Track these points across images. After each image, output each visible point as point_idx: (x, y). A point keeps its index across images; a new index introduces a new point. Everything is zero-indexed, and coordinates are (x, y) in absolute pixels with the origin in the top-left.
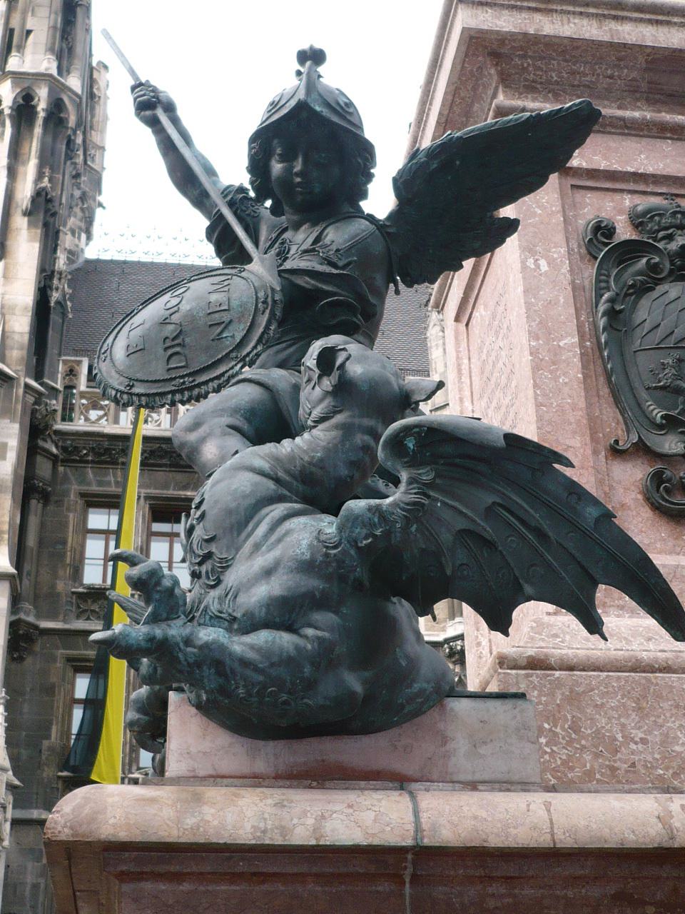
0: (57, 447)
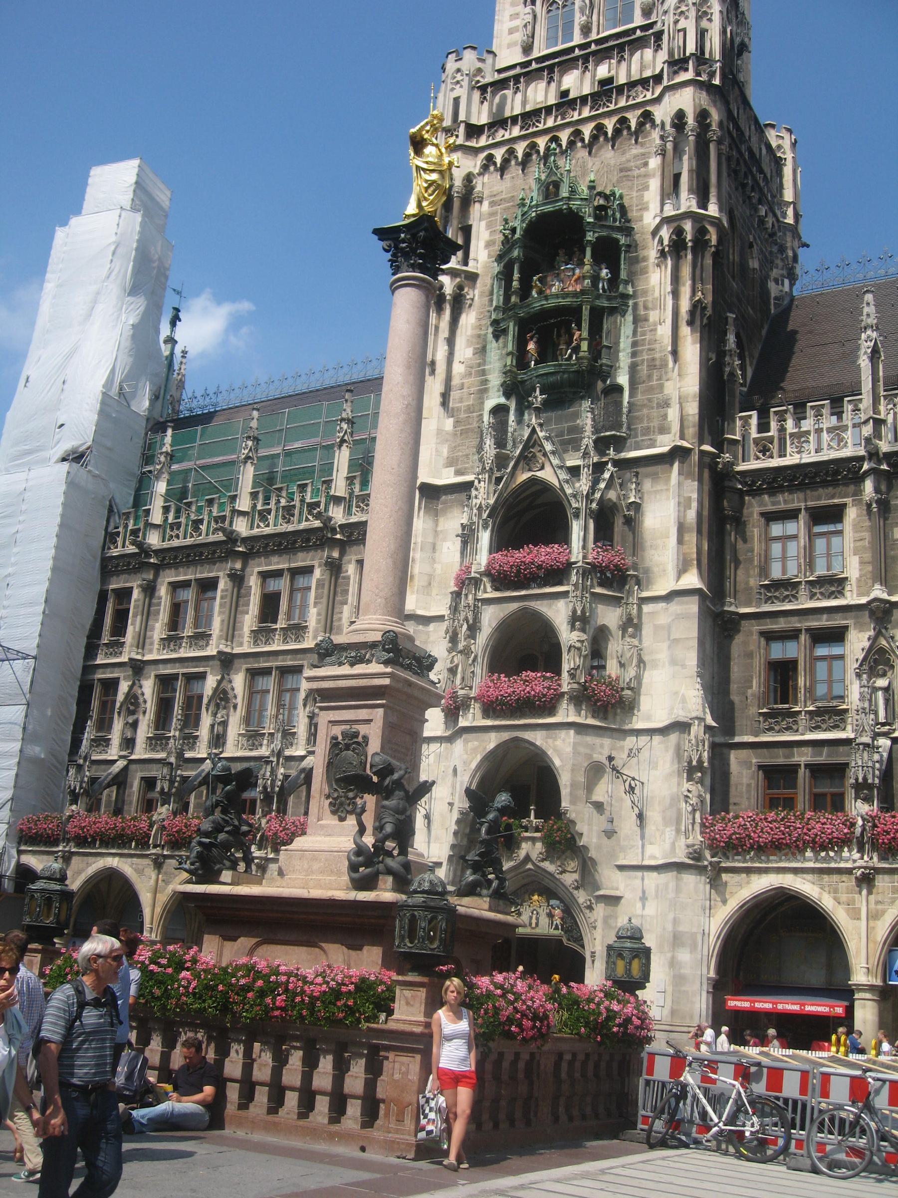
0: (741, 483)
